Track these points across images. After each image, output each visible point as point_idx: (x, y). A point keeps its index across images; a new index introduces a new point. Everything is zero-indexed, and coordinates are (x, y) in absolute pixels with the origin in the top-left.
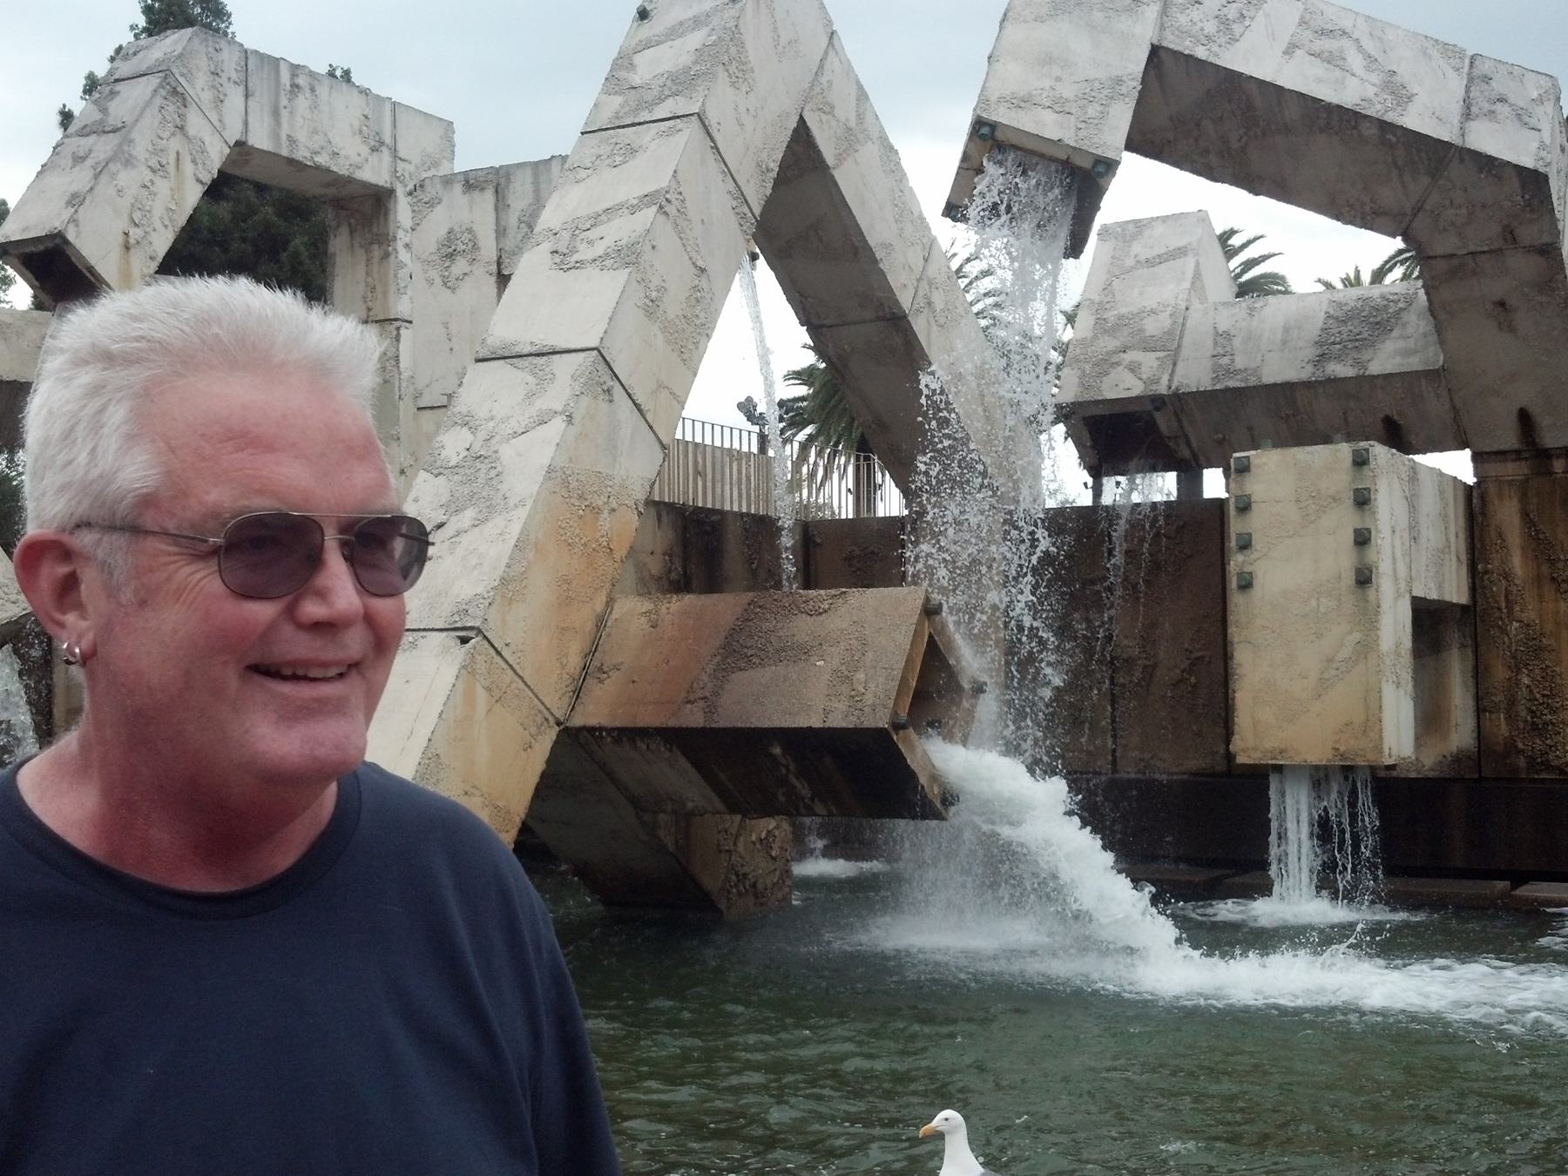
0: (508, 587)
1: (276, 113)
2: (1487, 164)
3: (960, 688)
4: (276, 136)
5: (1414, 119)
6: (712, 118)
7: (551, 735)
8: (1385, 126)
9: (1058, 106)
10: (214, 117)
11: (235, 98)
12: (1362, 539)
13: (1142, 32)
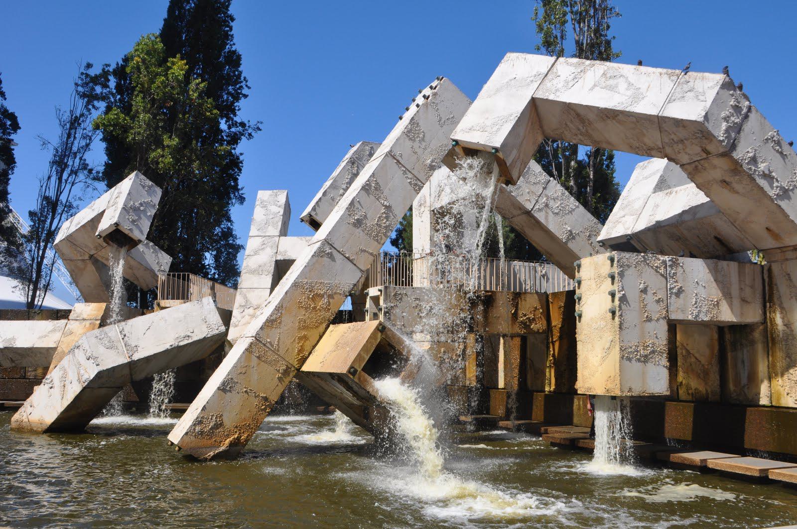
2: (679, 123)
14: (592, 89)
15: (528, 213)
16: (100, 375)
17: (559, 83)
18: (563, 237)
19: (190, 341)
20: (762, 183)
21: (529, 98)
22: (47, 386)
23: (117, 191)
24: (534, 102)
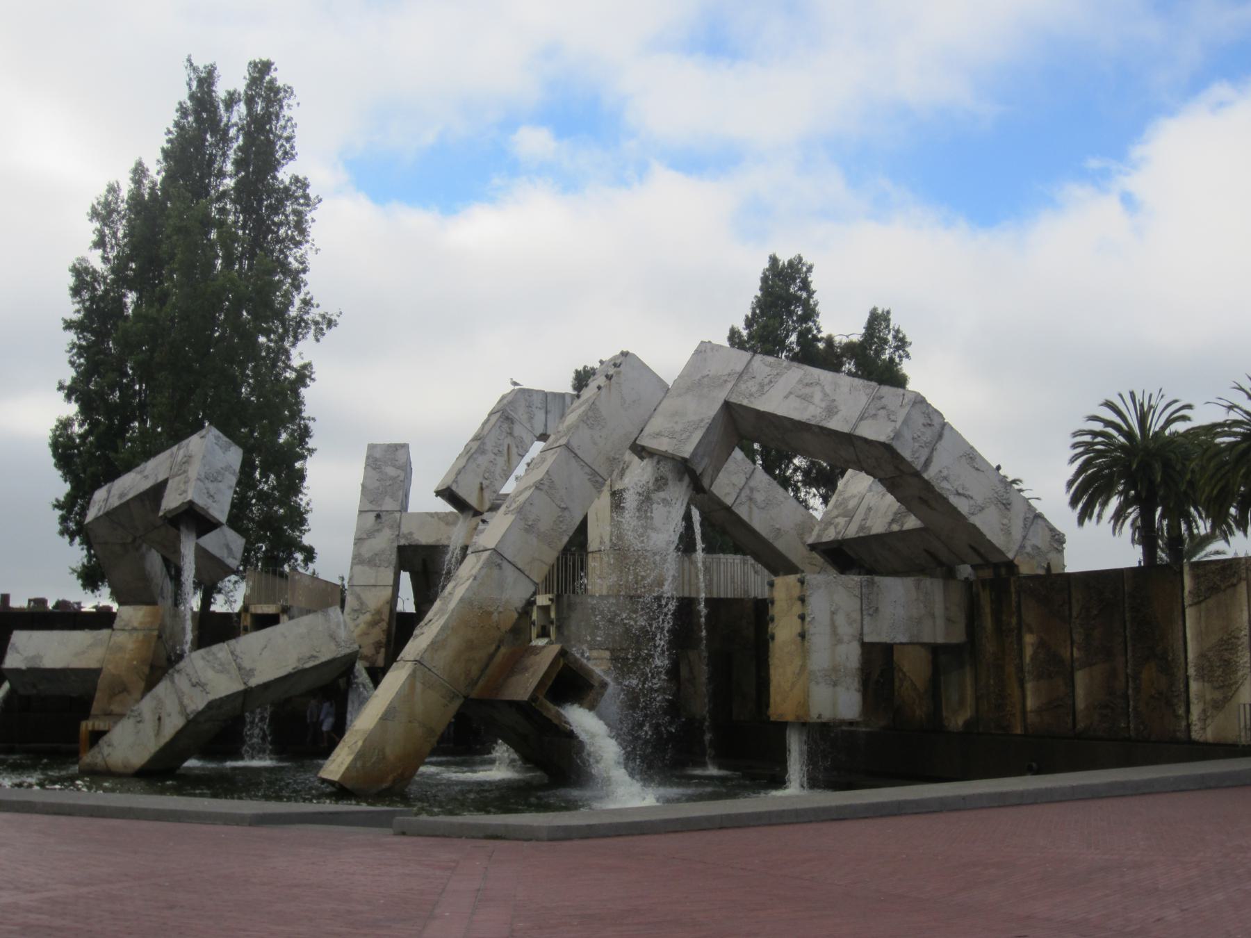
0: (434, 646)
3: (592, 686)
5: (835, 424)
6: (575, 444)
7: (461, 701)
8: (822, 429)
9: (672, 436)
10: (528, 426)
11: (540, 416)
12: (802, 617)
13: (720, 397)
14: (786, 397)
15: (728, 509)
16: (211, 705)
17: (752, 386)
19: (317, 662)
21: (721, 402)
22: (132, 721)
23: (181, 452)
24: (727, 405)
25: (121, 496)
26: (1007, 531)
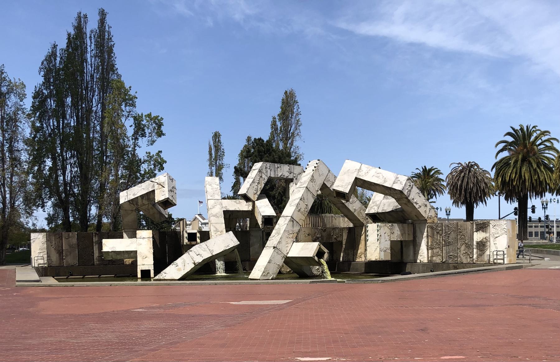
1: (275, 171)
4: (275, 174)
5: (386, 185)
6: (308, 187)
8: (383, 186)
11: (269, 171)
18: (353, 211)
20: (415, 204)
24: (356, 178)
25: (134, 195)
26: (425, 211)
